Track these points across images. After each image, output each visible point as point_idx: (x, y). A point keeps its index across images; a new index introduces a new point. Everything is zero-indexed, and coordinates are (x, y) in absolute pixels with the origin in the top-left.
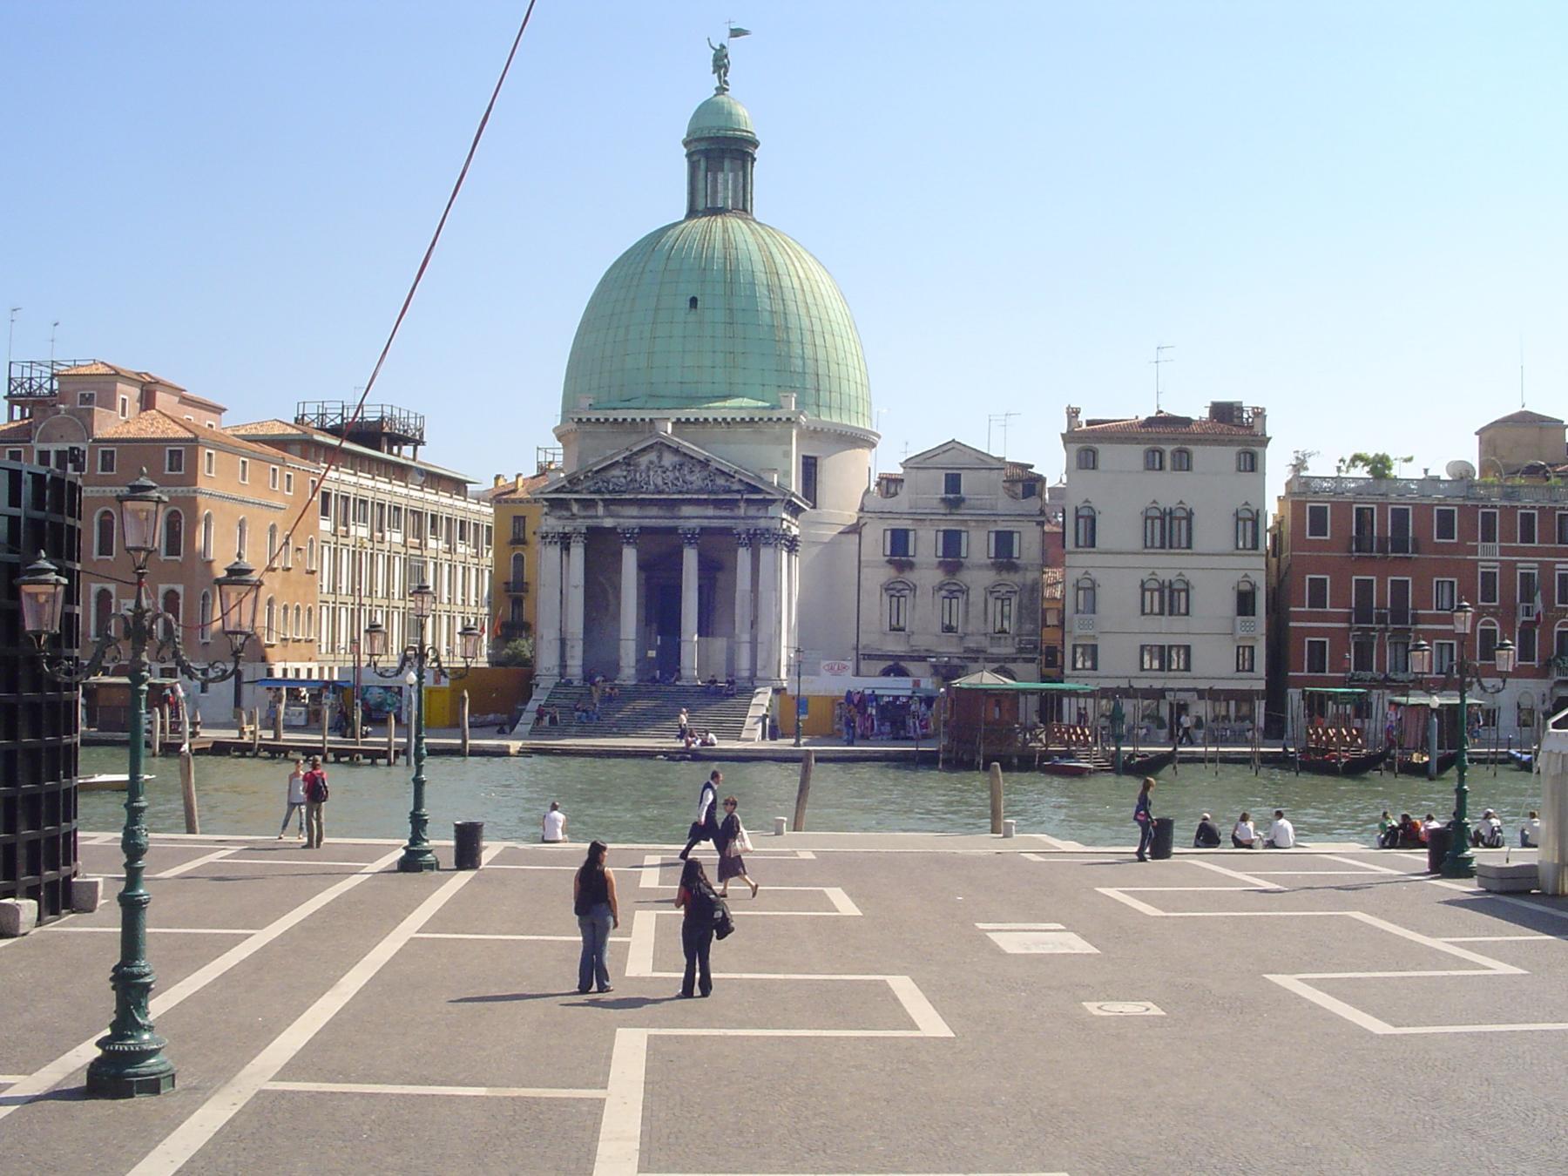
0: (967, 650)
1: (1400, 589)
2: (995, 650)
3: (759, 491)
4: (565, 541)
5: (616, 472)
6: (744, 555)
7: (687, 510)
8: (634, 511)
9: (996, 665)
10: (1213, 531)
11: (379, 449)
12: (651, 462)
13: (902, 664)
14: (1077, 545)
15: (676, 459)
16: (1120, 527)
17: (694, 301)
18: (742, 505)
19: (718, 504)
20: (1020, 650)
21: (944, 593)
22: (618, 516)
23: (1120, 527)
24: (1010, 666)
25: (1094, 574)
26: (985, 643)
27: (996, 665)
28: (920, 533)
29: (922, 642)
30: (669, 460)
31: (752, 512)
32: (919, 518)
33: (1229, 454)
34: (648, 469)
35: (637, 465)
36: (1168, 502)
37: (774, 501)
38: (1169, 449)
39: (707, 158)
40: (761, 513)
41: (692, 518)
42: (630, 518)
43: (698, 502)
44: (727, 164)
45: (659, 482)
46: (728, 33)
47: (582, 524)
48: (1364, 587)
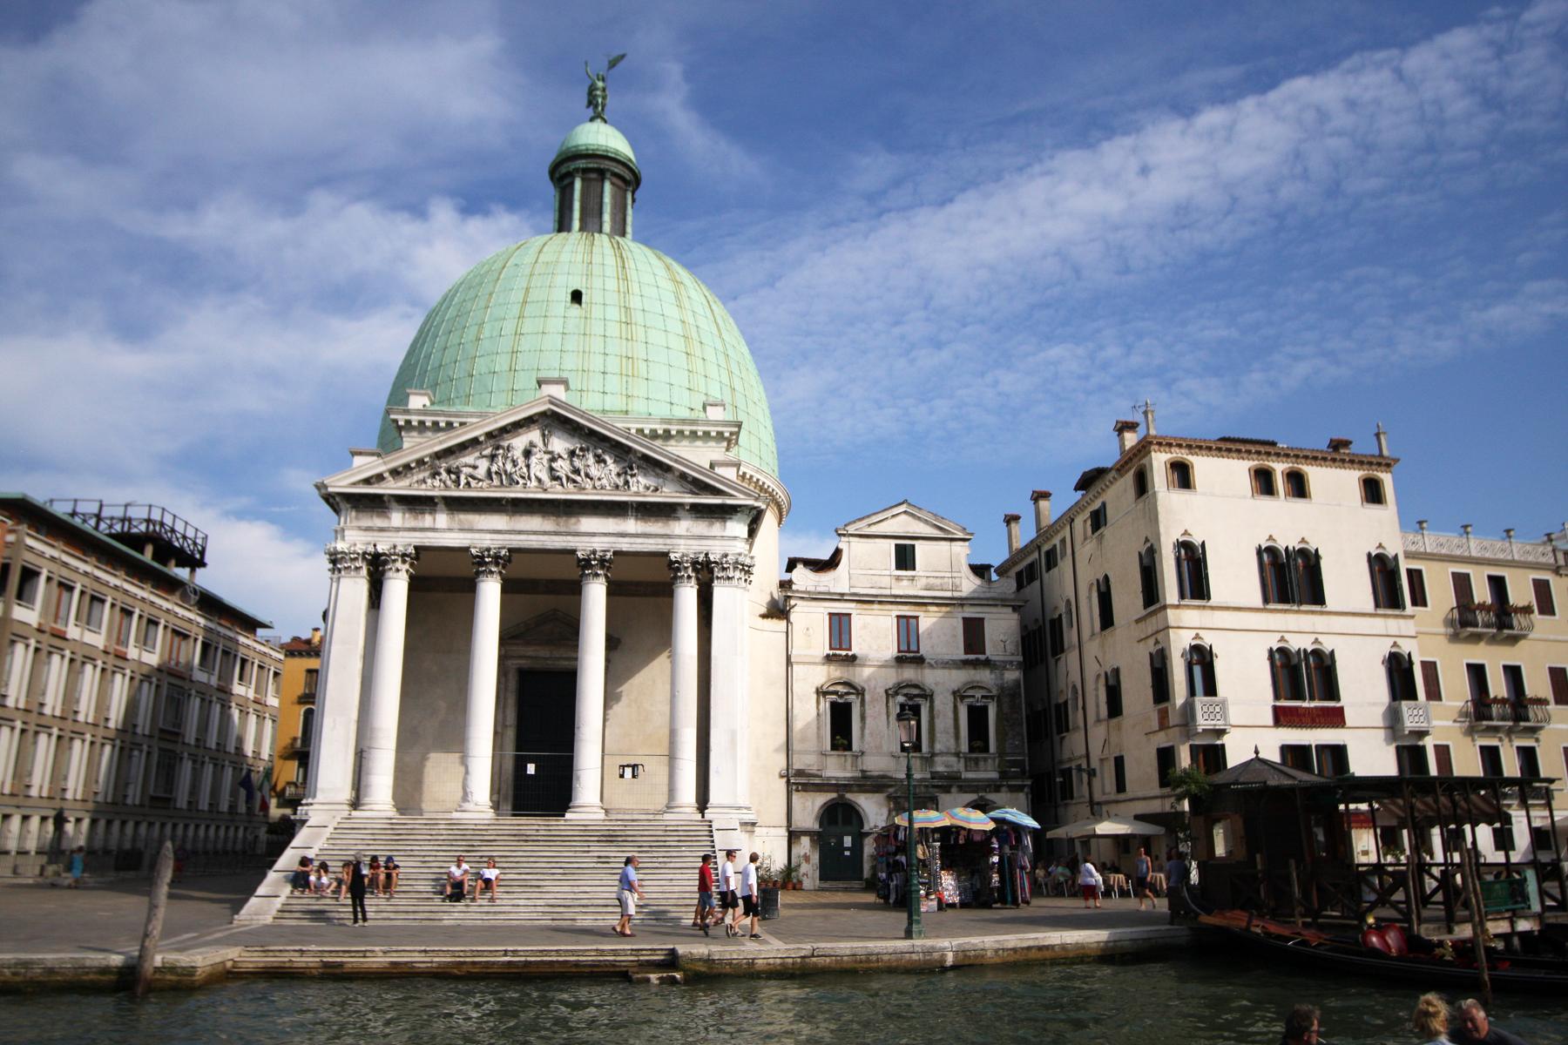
0: (935, 775)
1: (1514, 674)
2: (971, 775)
3: (717, 492)
4: (377, 566)
5: (469, 459)
6: (687, 596)
7: (588, 523)
8: (498, 521)
9: (973, 797)
10: (1347, 582)
11: (142, 552)
12: (532, 445)
13: (848, 796)
14: (1182, 596)
15: (574, 444)
16: (1235, 577)
17: (577, 297)
18: (680, 513)
19: (647, 510)
20: (1004, 775)
21: (901, 699)
22: (471, 530)
23: (1235, 577)
24: (991, 796)
25: (1208, 639)
26: (957, 766)
27: (973, 797)
29: (876, 764)
30: (560, 444)
32: (864, 601)
33: (1351, 479)
34: (527, 454)
36: (1287, 540)
38: (1279, 468)
39: (583, 180)
40: (716, 528)
41: (596, 535)
42: (487, 533)
44: (608, 187)
45: (545, 477)
46: (606, 64)
47: (407, 542)
48: (1477, 673)
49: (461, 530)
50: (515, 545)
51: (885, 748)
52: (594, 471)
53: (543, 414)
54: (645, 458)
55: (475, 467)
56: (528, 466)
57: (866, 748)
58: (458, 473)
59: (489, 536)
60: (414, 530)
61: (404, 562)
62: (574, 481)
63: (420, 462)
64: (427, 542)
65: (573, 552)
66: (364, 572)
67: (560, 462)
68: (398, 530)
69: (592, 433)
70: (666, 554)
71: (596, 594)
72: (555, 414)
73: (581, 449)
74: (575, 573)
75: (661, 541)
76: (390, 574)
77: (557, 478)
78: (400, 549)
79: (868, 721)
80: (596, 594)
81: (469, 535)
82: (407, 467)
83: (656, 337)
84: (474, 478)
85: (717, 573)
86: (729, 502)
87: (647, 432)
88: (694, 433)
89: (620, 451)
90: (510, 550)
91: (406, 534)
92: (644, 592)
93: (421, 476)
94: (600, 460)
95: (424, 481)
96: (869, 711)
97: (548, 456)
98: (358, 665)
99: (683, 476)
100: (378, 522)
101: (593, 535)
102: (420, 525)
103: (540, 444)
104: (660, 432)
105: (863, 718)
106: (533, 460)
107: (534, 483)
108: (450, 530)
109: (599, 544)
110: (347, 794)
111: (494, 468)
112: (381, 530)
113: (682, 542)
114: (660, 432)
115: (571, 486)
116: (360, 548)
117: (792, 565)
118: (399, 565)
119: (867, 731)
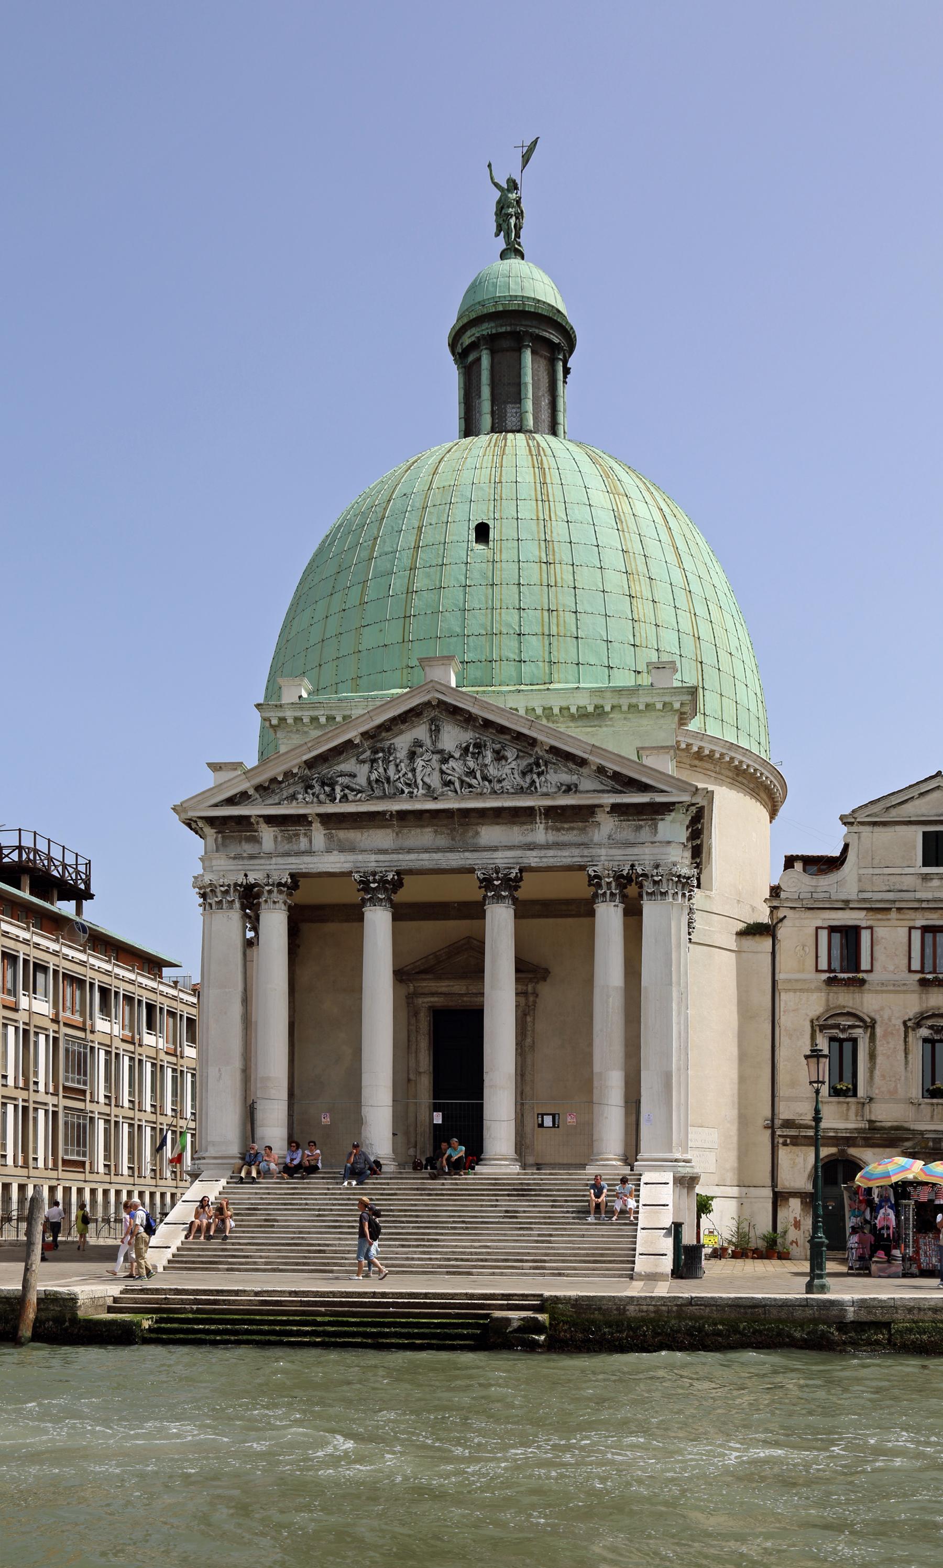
3: (645, 788)
5: (349, 765)
7: (489, 834)
8: (382, 838)
12: (418, 743)
18: (601, 817)
28: (880, 932)
29: (887, 1113)
30: (453, 737)
31: (626, 831)
34: (412, 755)
35: (390, 750)
37: (668, 808)
40: (645, 834)
43: (519, 816)
45: (435, 781)
47: (281, 869)
49: (342, 850)
50: (404, 866)
51: (901, 1093)
52: (492, 771)
53: (428, 704)
54: (554, 750)
55: (353, 776)
56: (413, 770)
57: (875, 1093)
58: (332, 785)
59: (373, 857)
60: (287, 854)
61: (280, 892)
62: (470, 786)
63: (288, 774)
64: (304, 868)
65: (471, 870)
66: (237, 905)
67: (452, 763)
68: (270, 856)
69: (488, 724)
70: (582, 868)
71: (500, 921)
72: (441, 703)
73: (477, 746)
74: (478, 895)
75: (576, 852)
76: (263, 906)
77: (448, 784)
78: (275, 878)
79: (880, 1060)
80: (500, 921)
81: (351, 857)
82: (274, 780)
83: (586, 578)
84: (352, 790)
85: (649, 887)
86: (660, 798)
87: (573, 710)
88: (633, 707)
89: (524, 742)
90: (398, 873)
91: (280, 860)
92: (557, 914)
93: (291, 791)
94: (499, 757)
95: (293, 797)
96: (880, 1048)
97: (436, 757)
98: (236, 1009)
99: (601, 770)
100: (248, 848)
101: (495, 849)
102: (295, 847)
103: (428, 742)
104: (590, 709)
105: (872, 1056)
106: (419, 763)
107: (421, 791)
108: (329, 851)
109: (501, 859)
110: (234, 1149)
111: (374, 777)
112: (252, 857)
113: (603, 852)
114: (590, 709)
115: (466, 791)
116: (230, 879)
117: (790, 862)
118: (275, 896)
119: (877, 1073)
